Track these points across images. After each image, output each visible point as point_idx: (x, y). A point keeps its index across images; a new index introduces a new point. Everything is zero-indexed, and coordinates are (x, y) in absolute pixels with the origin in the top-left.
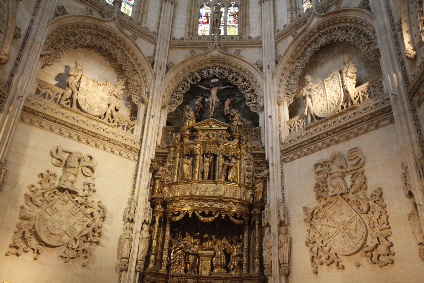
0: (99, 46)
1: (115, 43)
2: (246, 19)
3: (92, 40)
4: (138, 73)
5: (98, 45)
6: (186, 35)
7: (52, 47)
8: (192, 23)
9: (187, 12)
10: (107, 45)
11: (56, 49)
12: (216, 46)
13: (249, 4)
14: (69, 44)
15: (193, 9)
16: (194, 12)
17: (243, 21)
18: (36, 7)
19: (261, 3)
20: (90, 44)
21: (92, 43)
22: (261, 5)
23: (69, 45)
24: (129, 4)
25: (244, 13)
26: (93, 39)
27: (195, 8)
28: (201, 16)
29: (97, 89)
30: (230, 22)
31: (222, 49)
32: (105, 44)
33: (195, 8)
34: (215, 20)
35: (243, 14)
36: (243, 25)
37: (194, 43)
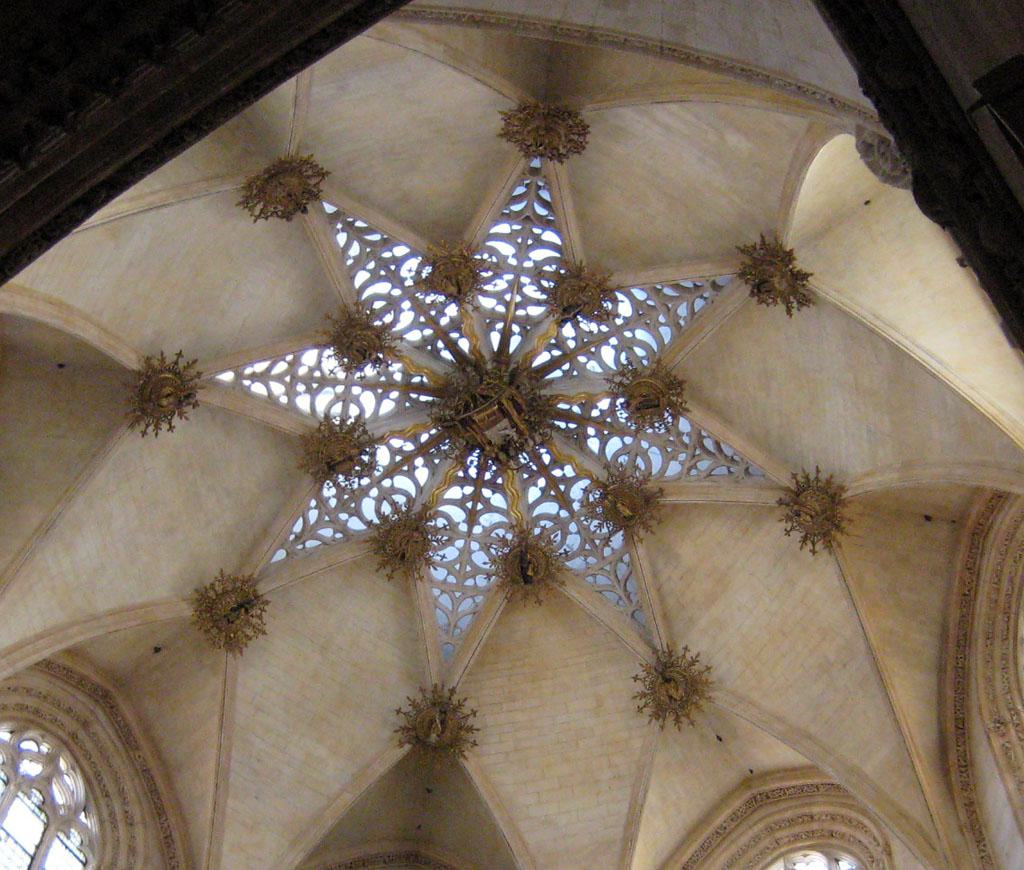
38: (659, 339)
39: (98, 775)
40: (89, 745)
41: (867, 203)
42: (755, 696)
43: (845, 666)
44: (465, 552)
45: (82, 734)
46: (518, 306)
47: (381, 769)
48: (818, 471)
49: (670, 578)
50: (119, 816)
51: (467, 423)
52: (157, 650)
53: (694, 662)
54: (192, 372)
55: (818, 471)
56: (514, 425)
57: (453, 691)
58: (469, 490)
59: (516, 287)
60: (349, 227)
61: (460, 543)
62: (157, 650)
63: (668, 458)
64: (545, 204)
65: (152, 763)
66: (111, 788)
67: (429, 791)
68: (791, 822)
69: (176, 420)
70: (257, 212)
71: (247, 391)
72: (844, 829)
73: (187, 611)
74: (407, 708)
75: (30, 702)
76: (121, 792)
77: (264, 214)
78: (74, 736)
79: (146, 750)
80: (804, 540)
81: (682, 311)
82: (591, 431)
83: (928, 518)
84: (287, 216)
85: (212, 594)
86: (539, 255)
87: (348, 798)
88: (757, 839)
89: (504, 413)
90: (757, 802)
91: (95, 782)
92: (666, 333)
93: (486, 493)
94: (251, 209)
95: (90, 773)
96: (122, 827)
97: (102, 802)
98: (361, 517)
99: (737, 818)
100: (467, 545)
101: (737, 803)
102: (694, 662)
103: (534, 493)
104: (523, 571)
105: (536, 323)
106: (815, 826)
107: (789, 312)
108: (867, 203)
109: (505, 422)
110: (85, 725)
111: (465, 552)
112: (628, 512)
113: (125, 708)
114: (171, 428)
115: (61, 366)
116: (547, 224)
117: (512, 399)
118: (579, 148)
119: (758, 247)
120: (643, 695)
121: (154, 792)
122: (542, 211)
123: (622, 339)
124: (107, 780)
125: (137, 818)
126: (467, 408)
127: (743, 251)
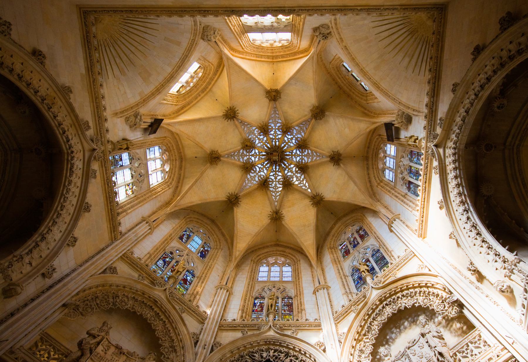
0: (139, 314)
1: (158, 314)
2: (301, 306)
3: (134, 305)
4: (175, 351)
5: (139, 312)
6: (239, 318)
7: (84, 302)
8: (245, 309)
9: (242, 300)
10: (148, 314)
11: (87, 305)
12: (270, 326)
13: (303, 294)
14: (105, 304)
15: (247, 298)
16: (249, 301)
17: (298, 309)
18: (86, 261)
19: (315, 293)
20: (130, 309)
21: (133, 308)
22: (316, 295)
23: (104, 305)
24: (184, 288)
25: (299, 302)
26: (135, 305)
27: (249, 298)
28: (256, 306)
29: (117, 359)
30: (285, 310)
31: (278, 330)
32: (147, 313)
33: (249, 298)
34: (270, 304)
35: (298, 303)
36: (298, 312)
37: (246, 325)
38: (308, 160)
39: (172, 169)
40: (174, 163)
42: (289, 225)
44: (255, 176)
45: (174, 161)
46: (262, 168)
47: (220, 199)
50: (172, 177)
51: (271, 154)
53: (282, 214)
56: (278, 159)
57: (239, 196)
58: (262, 167)
59: (292, 139)
61: (255, 174)
62: (196, 157)
63: (297, 180)
64: (306, 128)
65: (182, 174)
66: (173, 172)
68: (281, 251)
69: (229, 120)
72: (290, 256)
73: (208, 152)
74: (230, 193)
75: (171, 148)
76: (174, 175)
77: (267, 97)
78: (173, 160)
79: (182, 172)
80: (312, 204)
81: (314, 158)
82: (287, 169)
84: (270, 100)
86: (299, 136)
87: (213, 200)
88: (273, 251)
90: (277, 245)
92: (310, 160)
93: (264, 169)
96: (171, 179)
97: (170, 173)
98: (243, 159)
99: (271, 246)
100: (256, 175)
101: (272, 243)
102: (282, 214)
103: (272, 174)
104: (264, 183)
105: (291, 147)
106: (285, 254)
109: (277, 157)
110: (176, 160)
111: (255, 176)
113: (184, 162)
114: (227, 121)
116: (304, 131)
118: (321, 119)
120: (270, 215)
121: (180, 178)
122: (305, 129)
123: (302, 157)
125: (175, 180)
126: (273, 151)
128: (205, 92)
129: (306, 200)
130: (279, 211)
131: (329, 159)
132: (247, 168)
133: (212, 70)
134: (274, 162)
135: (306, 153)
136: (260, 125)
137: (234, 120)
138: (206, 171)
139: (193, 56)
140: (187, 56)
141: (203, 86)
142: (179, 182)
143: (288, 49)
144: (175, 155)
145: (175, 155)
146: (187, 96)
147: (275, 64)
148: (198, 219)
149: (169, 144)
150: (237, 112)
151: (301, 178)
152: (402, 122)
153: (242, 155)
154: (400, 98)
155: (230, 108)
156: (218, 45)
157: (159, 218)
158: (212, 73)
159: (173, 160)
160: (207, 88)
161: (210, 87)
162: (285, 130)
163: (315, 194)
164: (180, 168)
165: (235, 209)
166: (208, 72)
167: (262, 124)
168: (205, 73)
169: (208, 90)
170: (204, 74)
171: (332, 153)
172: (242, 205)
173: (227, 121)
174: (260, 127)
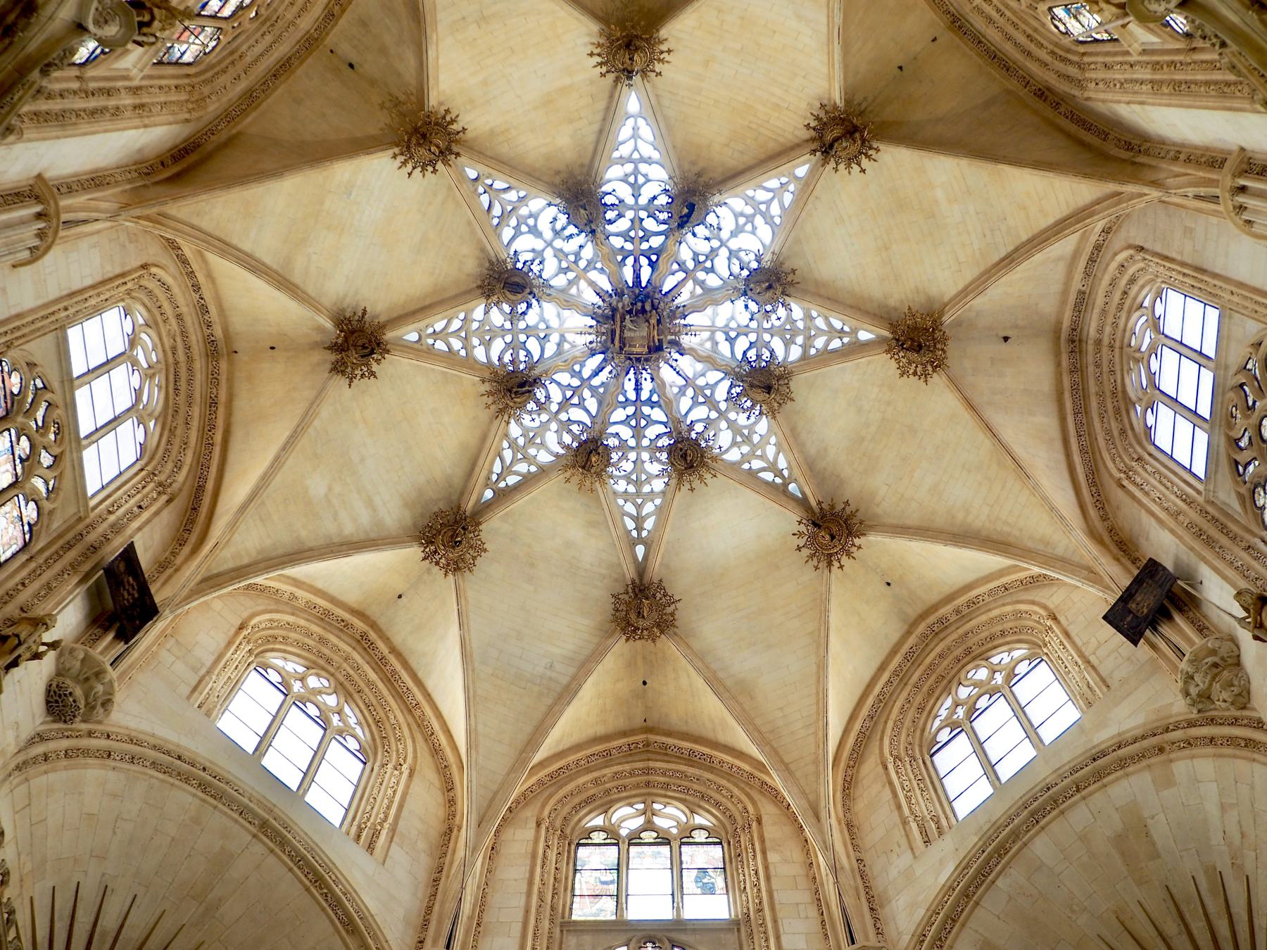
40: (1108, 329)
41: (272, 348)
43: (464, 18)
45: (1106, 341)
48: (410, 174)
49: (590, 124)
52: (1006, 339)
54: (802, 528)
55: (410, 174)
56: (622, 328)
59: (565, 404)
60: (639, 529)
67: (900, 68)
70: (673, 607)
71: (789, 468)
74: (855, 168)
75: (1110, 406)
76: (1113, 283)
79: (1076, 285)
80: (453, 121)
83: (351, 66)
85: (919, 369)
89: (623, 342)
91: (1126, 307)
94: (672, 614)
95: (1124, 315)
104: (689, 215)
107: (365, 311)
108: (272, 348)
109: (627, 334)
110: (1098, 342)
112: (582, 211)
113: (1066, 323)
115: (889, 584)
117: (613, 341)
119: (358, 377)
120: (659, 60)
124: (1117, 296)
127: (373, 374)
128: (932, 619)
129: (488, 127)
130: (617, 80)
131: (390, 335)
132: (770, 287)
133: (890, 724)
134: (643, 311)
135: (498, 346)
136: (708, 476)
137: (819, 503)
138: (960, 287)
139: (943, 879)
140: (966, 894)
141: (938, 650)
142: (1098, 248)
143: (584, 796)
144: (1098, 365)
145: (1098, 365)
146: (1007, 626)
147: (638, 722)
148: (1029, 54)
149: (1116, 433)
150: (802, 542)
151: (517, 228)
152: (87, 679)
153: (795, 332)
154: (111, 775)
155: (830, 564)
156: (844, 910)
157: (1197, 197)
158: (896, 710)
159: (1111, 347)
160: (924, 636)
161: (912, 641)
162: (594, 459)
163: (440, 166)
164: (1082, 301)
165: (837, 98)
166: (911, 714)
167: (696, 484)
168: (921, 709)
169: (922, 628)
170: (926, 710)
171: (375, 367)
172: (803, 105)
173: (847, 503)
174: (704, 464)
